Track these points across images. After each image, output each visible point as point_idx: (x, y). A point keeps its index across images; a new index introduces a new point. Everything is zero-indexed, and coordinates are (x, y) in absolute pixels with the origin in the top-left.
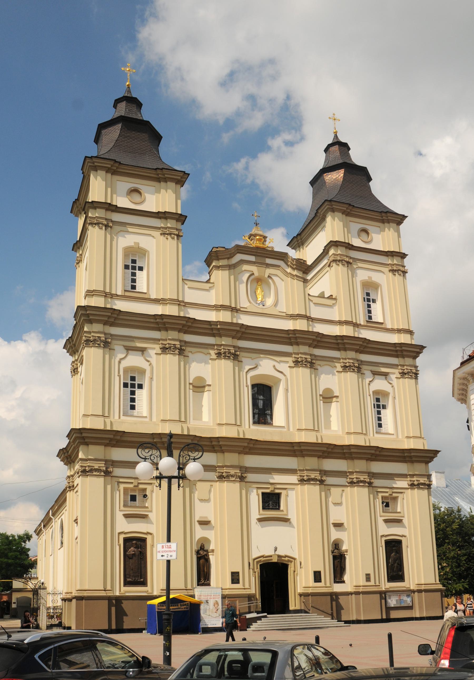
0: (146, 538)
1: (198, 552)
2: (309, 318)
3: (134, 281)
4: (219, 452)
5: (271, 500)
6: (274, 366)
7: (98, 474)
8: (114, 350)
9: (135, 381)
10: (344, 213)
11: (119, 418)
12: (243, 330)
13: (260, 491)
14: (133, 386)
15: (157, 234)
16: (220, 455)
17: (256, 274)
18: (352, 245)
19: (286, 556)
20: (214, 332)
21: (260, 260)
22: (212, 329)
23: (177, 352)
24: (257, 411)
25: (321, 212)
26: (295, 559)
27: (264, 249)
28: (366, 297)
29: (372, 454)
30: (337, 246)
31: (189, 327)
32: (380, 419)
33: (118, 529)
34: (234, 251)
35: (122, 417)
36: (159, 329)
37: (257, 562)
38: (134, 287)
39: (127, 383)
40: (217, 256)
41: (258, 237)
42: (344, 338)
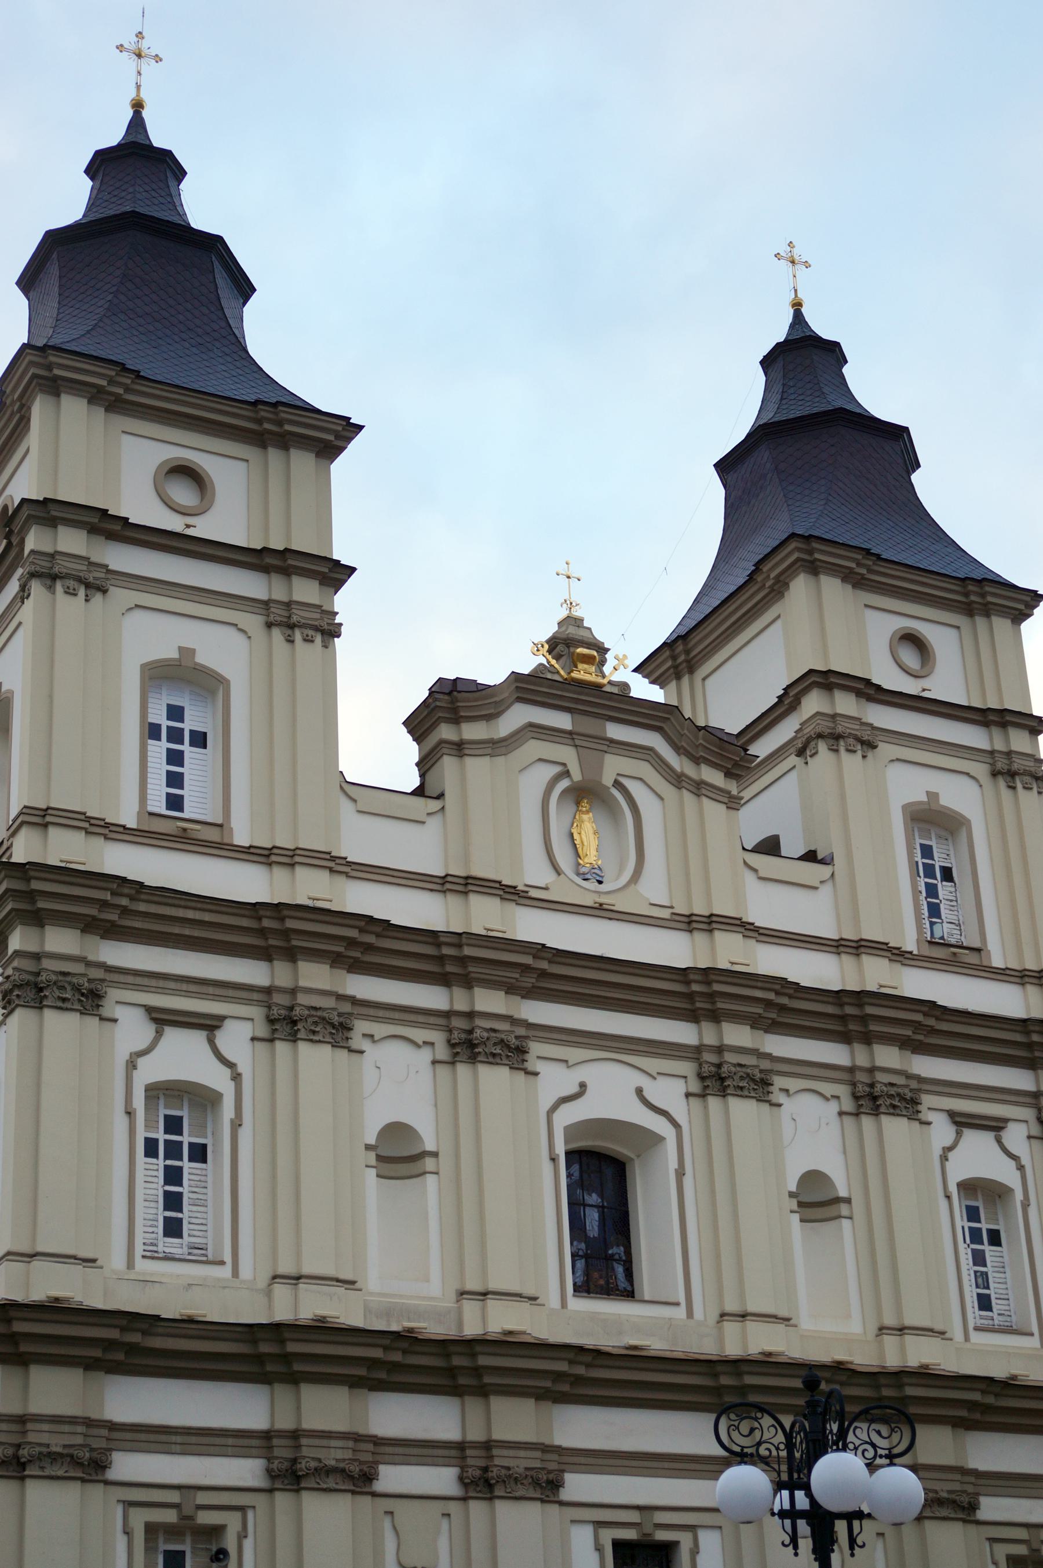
3: (175, 780)
6: (639, 1091)
7: (60, 1473)
8: (115, 1021)
9: (181, 1134)
11: (130, 1264)
12: (544, 965)
13: (608, 1536)
14: (173, 1150)
15: (253, 622)
16: (473, 1404)
18: (878, 688)
20: (450, 968)
21: (589, 725)
22: (441, 959)
24: (583, 1246)
25: (772, 570)
27: (598, 687)
29: (972, 1405)
31: (369, 948)
32: (982, 1280)
34: (506, 695)
35: (143, 1266)
36: (265, 954)
38: (175, 802)
40: (455, 710)
41: (580, 650)
42: (866, 1000)
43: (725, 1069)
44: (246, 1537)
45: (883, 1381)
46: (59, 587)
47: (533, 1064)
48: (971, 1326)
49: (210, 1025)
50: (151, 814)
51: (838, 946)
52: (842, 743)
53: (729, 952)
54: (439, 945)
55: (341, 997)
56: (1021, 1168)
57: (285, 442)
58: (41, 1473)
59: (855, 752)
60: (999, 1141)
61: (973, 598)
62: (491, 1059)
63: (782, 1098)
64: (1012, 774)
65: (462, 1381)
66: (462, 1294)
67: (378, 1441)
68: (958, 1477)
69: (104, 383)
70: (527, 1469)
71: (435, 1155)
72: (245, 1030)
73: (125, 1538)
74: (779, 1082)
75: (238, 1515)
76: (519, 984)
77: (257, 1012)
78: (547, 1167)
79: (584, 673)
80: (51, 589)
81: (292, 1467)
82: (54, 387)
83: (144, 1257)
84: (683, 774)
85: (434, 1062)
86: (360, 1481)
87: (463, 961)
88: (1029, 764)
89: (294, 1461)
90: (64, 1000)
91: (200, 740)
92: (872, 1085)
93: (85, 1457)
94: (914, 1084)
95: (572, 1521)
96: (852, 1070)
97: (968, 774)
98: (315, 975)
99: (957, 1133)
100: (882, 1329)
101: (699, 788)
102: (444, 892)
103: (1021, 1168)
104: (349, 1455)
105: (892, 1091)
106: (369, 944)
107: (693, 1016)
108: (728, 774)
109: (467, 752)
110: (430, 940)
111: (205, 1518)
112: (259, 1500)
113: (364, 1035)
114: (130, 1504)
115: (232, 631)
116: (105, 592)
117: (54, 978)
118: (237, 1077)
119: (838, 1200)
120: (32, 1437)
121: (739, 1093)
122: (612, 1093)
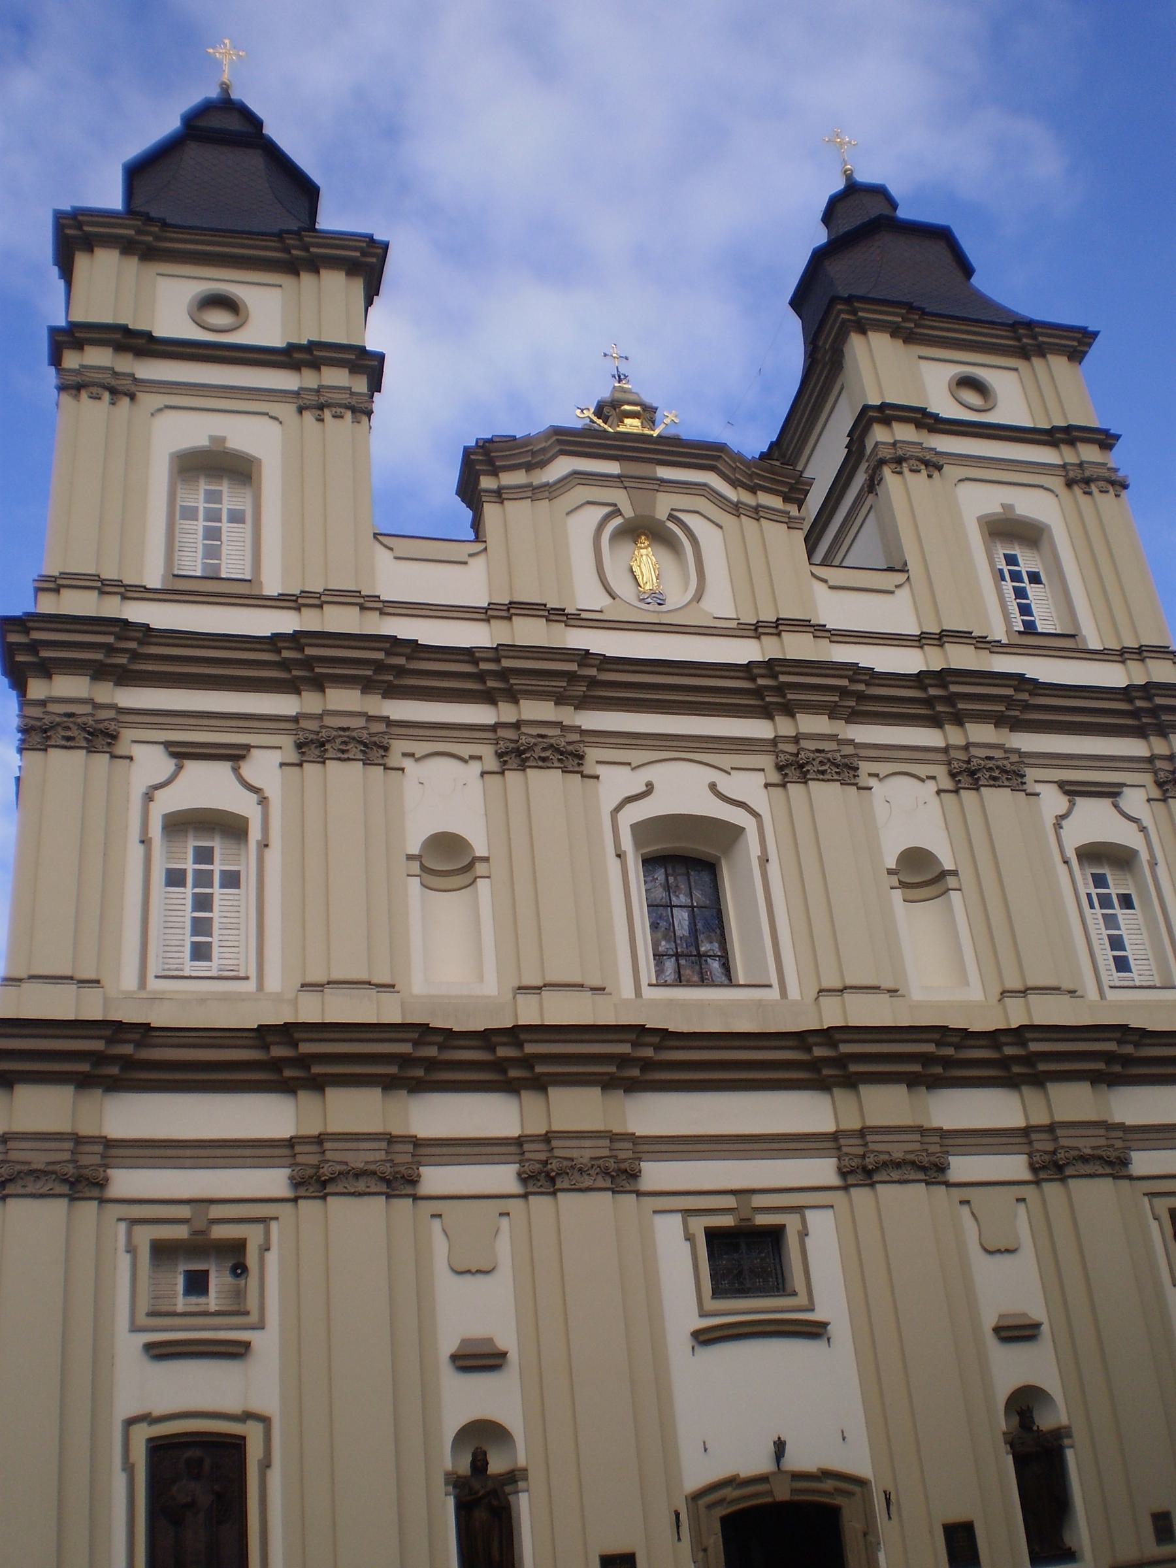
0: (244, 1438)
1: (457, 1483)
2: (820, 631)
4: (527, 1088)
5: (747, 1255)
6: (713, 787)
7: (44, 1190)
8: (131, 758)
9: (212, 864)
10: (895, 332)
11: (143, 983)
12: (593, 672)
13: (699, 1225)
15: (287, 411)
17: (628, 512)
18: (935, 417)
19: (826, 1474)
20: (491, 684)
22: (481, 677)
23: (355, 751)
26: (861, 1482)
28: (1006, 569)
29: (1109, 1057)
30: (887, 422)
31: (401, 671)
32: (1116, 943)
33: (126, 1407)
36: (292, 687)
37: (710, 1507)
39: (183, 872)
40: (490, 461)
41: (627, 407)
43: (802, 755)
44: (268, 1249)
45: (1003, 1039)
46: (84, 395)
47: (590, 767)
48: (1106, 984)
49: (235, 755)
50: (174, 576)
51: (920, 640)
52: (904, 465)
53: (798, 647)
54: (476, 662)
55: (370, 718)
56: (1143, 829)
57: (314, 265)
58: (21, 1191)
59: (919, 471)
60: (1116, 806)
61: (1025, 340)
62: (541, 764)
63: (872, 782)
64: (1087, 481)
65: (513, 1073)
66: (519, 988)
67: (417, 1143)
68: (1102, 1132)
69: (132, 232)
70: (592, 1159)
71: (486, 859)
72: (276, 757)
73: (128, 1257)
74: (865, 767)
75: (260, 1227)
76: (568, 693)
77: (287, 741)
78: (613, 864)
79: (632, 425)
80: (77, 397)
81: (318, 1173)
82: (89, 244)
83: (157, 977)
84: (739, 502)
85: (483, 774)
86: (397, 1182)
87: (504, 674)
88: (1103, 472)
89: (318, 1167)
90: (69, 739)
91: (236, 517)
92: (968, 762)
93: (79, 1175)
94: (1014, 758)
95: (655, 1212)
96: (946, 750)
97: (1042, 487)
98: (345, 700)
99: (1070, 801)
100: (1004, 993)
101: (757, 513)
102: (488, 621)
103: (1143, 829)
104: (381, 1155)
105: (990, 764)
106: (397, 667)
107: (766, 713)
108: (786, 499)
109: (504, 496)
110: (466, 658)
111: (220, 1232)
112: (286, 1210)
113: (405, 755)
114: (134, 1222)
115: (266, 419)
116: (132, 397)
117: (58, 719)
118: (263, 801)
119: (944, 874)
120: (14, 1156)
121: (821, 777)
122: (683, 790)
